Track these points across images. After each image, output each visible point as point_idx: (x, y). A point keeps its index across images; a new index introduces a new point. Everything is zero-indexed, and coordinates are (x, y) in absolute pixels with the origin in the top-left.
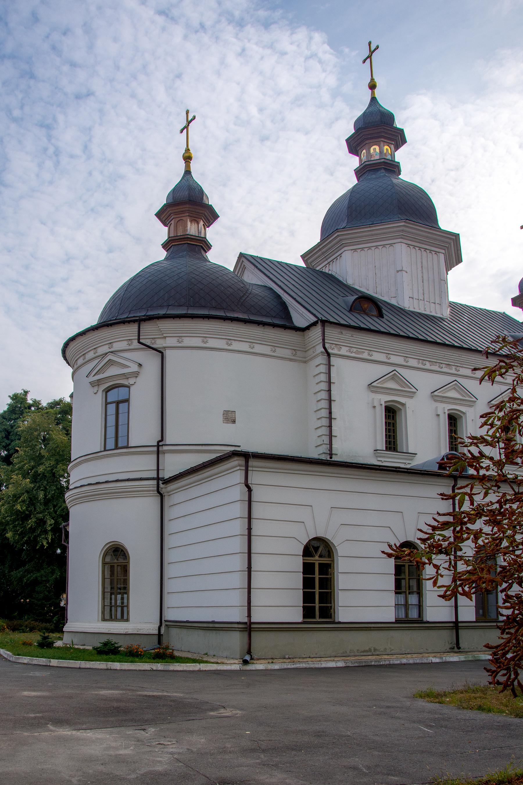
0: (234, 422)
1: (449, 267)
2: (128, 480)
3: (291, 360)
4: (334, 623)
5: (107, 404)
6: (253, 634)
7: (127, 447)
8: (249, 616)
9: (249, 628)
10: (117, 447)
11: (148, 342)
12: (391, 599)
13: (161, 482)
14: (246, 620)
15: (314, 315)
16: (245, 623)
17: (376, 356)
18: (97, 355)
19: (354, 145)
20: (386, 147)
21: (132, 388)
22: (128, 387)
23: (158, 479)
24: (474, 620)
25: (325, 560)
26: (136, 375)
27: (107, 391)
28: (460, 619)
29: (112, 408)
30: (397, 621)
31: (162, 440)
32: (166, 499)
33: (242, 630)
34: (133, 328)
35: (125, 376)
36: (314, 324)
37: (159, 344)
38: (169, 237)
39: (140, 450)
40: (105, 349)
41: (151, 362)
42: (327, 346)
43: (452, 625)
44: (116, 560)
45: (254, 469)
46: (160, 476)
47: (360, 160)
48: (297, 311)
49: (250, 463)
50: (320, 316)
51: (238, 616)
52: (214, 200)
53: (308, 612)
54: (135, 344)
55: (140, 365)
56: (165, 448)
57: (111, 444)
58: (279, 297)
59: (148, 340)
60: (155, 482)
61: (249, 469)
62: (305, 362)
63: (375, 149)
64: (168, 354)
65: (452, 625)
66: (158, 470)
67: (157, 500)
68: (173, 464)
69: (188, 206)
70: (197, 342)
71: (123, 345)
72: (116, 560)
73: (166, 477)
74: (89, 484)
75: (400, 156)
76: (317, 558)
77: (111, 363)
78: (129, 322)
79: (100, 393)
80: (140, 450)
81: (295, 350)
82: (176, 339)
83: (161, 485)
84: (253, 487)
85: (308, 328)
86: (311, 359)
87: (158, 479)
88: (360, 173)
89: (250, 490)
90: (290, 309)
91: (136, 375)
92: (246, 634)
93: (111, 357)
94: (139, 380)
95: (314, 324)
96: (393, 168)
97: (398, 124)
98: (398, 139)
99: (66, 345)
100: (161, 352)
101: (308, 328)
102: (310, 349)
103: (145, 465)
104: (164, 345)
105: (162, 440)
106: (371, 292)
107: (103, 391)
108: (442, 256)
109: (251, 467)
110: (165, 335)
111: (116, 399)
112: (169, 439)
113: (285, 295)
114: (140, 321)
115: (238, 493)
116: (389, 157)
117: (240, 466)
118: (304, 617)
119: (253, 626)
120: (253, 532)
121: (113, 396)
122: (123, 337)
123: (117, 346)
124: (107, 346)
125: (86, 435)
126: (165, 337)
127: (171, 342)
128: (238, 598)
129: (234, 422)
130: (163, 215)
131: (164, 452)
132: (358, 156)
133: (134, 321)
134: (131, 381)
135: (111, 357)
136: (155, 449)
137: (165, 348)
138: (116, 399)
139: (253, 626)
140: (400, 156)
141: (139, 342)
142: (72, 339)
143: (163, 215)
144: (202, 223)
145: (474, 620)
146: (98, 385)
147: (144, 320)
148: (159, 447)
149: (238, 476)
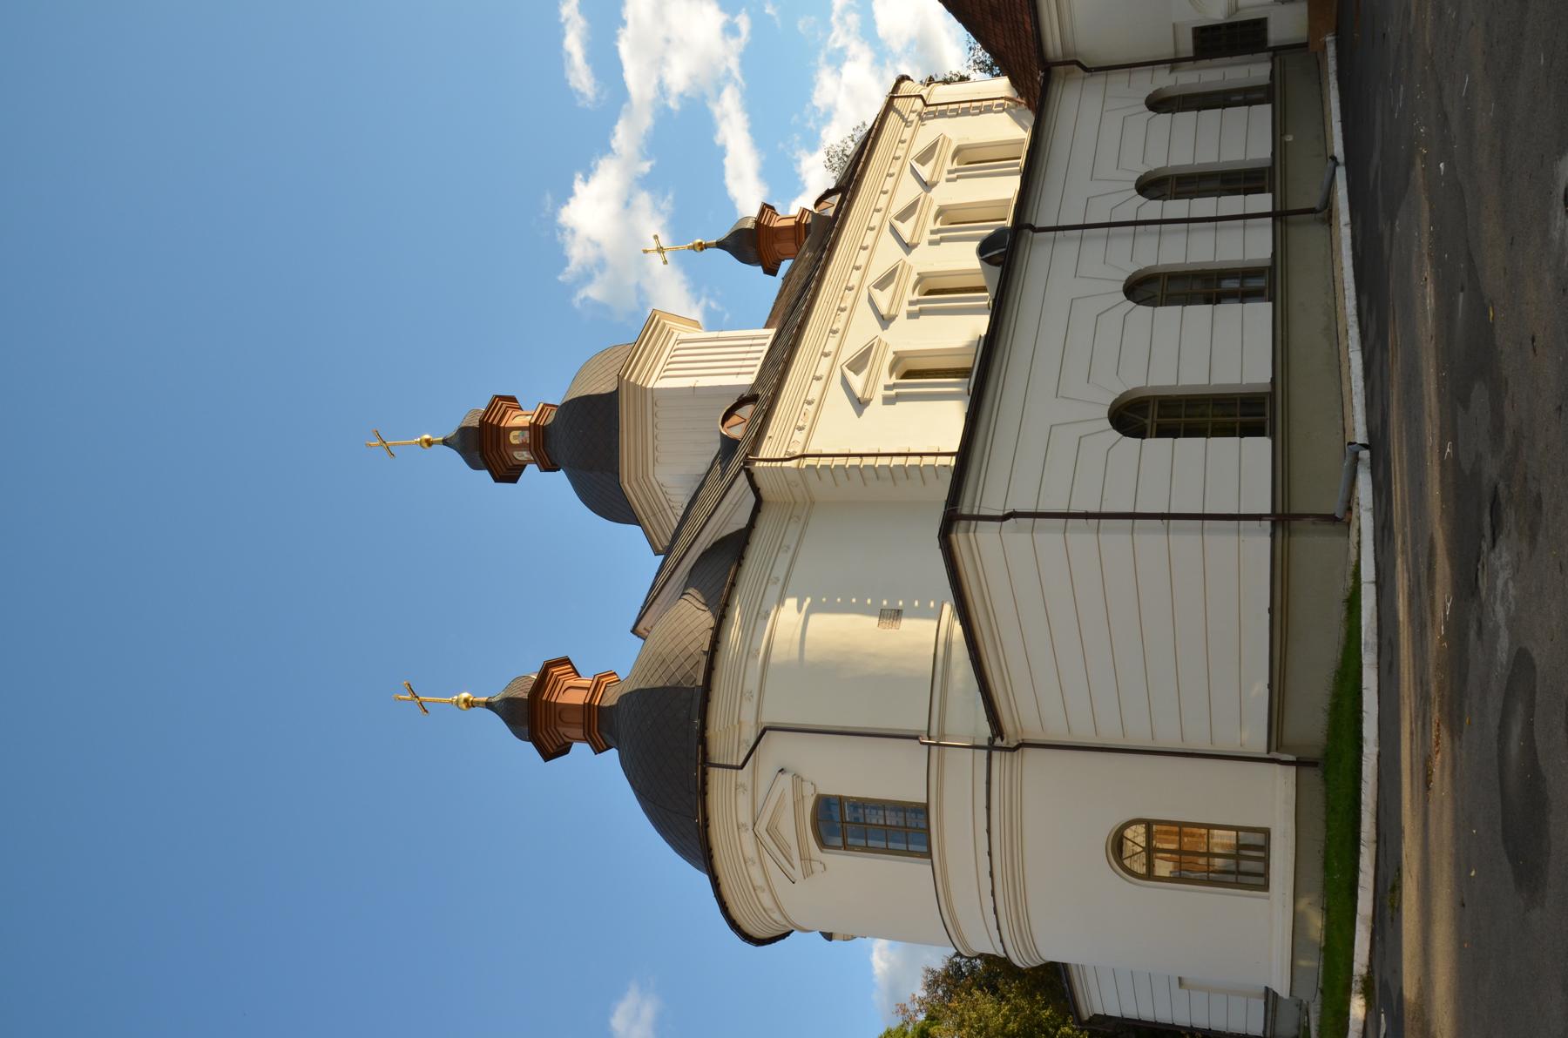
2: (988, 808)
3: (806, 524)
4: (1273, 394)
6: (1296, 509)
8: (1259, 517)
9: (1282, 520)
12: (1230, 311)
13: (998, 742)
14: (1267, 524)
15: (737, 476)
17: (814, 393)
19: (508, 473)
23: (991, 748)
24: (1270, 305)
25: (1153, 410)
26: (797, 778)
27: (823, 844)
28: (1269, 209)
30: (1272, 299)
33: (1289, 533)
34: (715, 776)
38: (586, 740)
40: (747, 837)
41: (777, 749)
43: (1278, 224)
46: (986, 743)
47: (530, 462)
49: (965, 511)
51: (1258, 542)
53: (1252, 430)
56: (934, 732)
58: (706, 555)
60: (996, 754)
64: (768, 718)
65: (1278, 224)
66: (974, 747)
67: (1029, 751)
68: (968, 720)
71: (744, 802)
76: (1148, 421)
77: (772, 831)
78: (705, 783)
82: (745, 703)
83: (1004, 744)
87: (991, 748)
88: (548, 466)
89: (1014, 515)
92: (1295, 524)
104: (753, 723)
112: (919, 724)
114: (706, 763)
115: (1017, 537)
117: (967, 531)
118: (1262, 435)
119: (1279, 510)
120: (1094, 509)
122: (731, 804)
123: (745, 817)
128: (1222, 539)
130: (552, 750)
131: (942, 735)
132: (524, 467)
133: (705, 774)
136: (934, 750)
143: (552, 750)
145: (1270, 305)
148: (931, 742)
149: (986, 535)
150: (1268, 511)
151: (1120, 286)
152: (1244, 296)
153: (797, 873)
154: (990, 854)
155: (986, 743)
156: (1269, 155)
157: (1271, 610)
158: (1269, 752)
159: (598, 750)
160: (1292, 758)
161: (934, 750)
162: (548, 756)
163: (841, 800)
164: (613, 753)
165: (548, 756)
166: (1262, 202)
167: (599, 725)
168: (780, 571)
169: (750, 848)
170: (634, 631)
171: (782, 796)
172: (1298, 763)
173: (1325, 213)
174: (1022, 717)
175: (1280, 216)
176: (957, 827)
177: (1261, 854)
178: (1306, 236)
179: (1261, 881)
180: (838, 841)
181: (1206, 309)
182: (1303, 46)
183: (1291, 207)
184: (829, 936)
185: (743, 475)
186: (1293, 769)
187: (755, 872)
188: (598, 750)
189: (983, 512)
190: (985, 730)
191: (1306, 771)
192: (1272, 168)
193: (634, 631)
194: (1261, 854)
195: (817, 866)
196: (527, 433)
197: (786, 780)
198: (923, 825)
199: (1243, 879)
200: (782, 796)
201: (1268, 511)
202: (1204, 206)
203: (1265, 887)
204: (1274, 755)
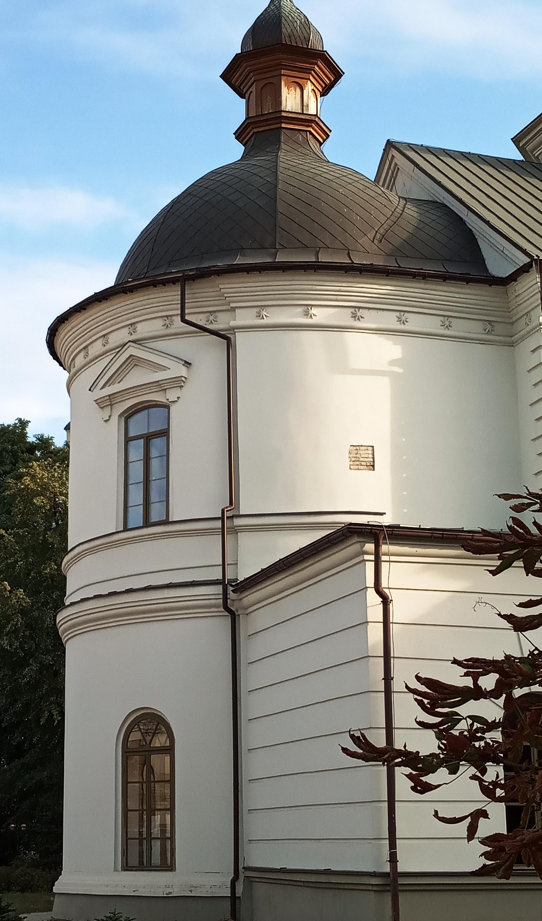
3: (482, 342)
5: (128, 440)
6: (402, 898)
7: (166, 522)
8: (393, 859)
10: (147, 523)
14: (387, 868)
15: (524, 252)
16: (386, 875)
18: (108, 347)
21: (174, 409)
22: (167, 407)
26: (178, 382)
27: (128, 415)
29: (137, 451)
32: (242, 622)
33: (380, 890)
34: (173, 294)
35: (160, 386)
36: (525, 269)
37: (221, 323)
39: (192, 527)
40: (122, 336)
41: (207, 356)
44: (146, 742)
45: (393, 558)
48: (493, 246)
49: (384, 548)
50: (534, 252)
51: (369, 859)
52: (333, 44)
54: (178, 325)
55: (187, 364)
56: (238, 522)
57: (136, 516)
59: (202, 316)
60: (219, 589)
61: (384, 558)
62: (512, 345)
64: (241, 340)
68: (255, 554)
69: (275, 55)
70: (294, 316)
72: (146, 742)
73: (241, 578)
74: (96, 597)
77: (133, 362)
78: (164, 283)
79: (115, 419)
80: (192, 527)
81: (490, 322)
83: (232, 595)
84: (392, 594)
85: (513, 277)
86: (523, 338)
90: (480, 242)
91: (178, 382)
93: (133, 350)
94: (186, 393)
95: (525, 269)
100: (226, 338)
101: (513, 277)
102: (522, 317)
103: (198, 556)
104: (233, 323)
107: (120, 416)
109: (385, 554)
110: (232, 305)
111: (146, 431)
114: (183, 281)
119: (401, 881)
121: (138, 426)
124: (126, 330)
125: (91, 502)
126: (233, 309)
127: (244, 318)
131: (235, 531)
133: (174, 281)
134: (172, 395)
135: (133, 350)
136: (219, 524)
137: (233, 329)
138: (146, 431)
139: (401, 881)
141: (184, 321)
142: (62, 320)
144: (309, 87)
146: (111, 405)
147: (193, 278)
148: (228, 522)
150: (401, 868)
153: (99, 393)
154: (129, 591)
155: (229, 576)
157: (328, 872)
158: (246, 869)
159: (240, 135)
160: (239, 891)
161: (219, 524)
162: (226, 76)
164: (235, 151)
165: (226, 76)
167: (263, 130)
168: (415, 322)
169: (115, 339)
170: (390, 144)
172: (234, 898)
174: (264, 614)
177: (156, 859)
179: (134, 860)
184: (67, 428)
186: (227, 893)
187: (97, 348)
188: (240, 135)
189: (384, 567)
190: (244, 573)
191: (228, 904)
193: (390, 144)
194: (156, 859)
195: (107, 411)
199: (134, 846)
201: (401, 868)
203: (127, 867)
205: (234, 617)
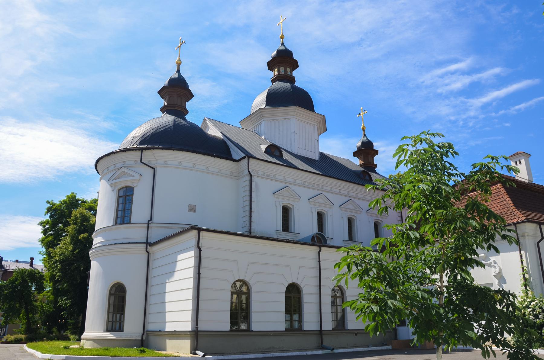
0: (195, 211)
1: (320, 133)
7: (130, 223)
11: (146, 162)
20: (288, 69)
30: (287, 330)
31: (151, 220)
36: (244, 158)
42: (250, 170)
46: (149, 241)
48: (234, 150)
56: (152, 225)
63: (282, 69)
75: (295, 73)
85: (240, 160)
93: (124, 169)
95: (244, 158)
96: (292, 80)
97: (295, 57)
98: (295, 65)
99: (98, 161)
101: (240, 160)
105: (151, 220)
106: (277, 144)
108: (316, 127)
112: (155, 219)
113: (229, 141)
114: (142, 150)
116: (289, 73)
129: (195, 211)
140: (295, 73)
142: (101, 158)
151: (294, 281)
152: (290, 321)
155: (149, 241)
156: (349, 328)
160: (144, 338)
163: (132, 195)
166: (328, 326)
171: (133, 176)
173: (322, 347)
175: (321, 332)
176: (127, 232)
178: (314, 341)
180: (121, 194)
181: (284, 309)
182: (396, 338)
183: (323, 336)
185: (244, 155)
186: (140, 339)
192: (345, 329)
196: (283, 73)
197: (137, 176)
198: (126, 222)
200: (133, 176)
202: (327, 308)
203: (107, 330)
204: (145, 333)
205: (148, 253)
